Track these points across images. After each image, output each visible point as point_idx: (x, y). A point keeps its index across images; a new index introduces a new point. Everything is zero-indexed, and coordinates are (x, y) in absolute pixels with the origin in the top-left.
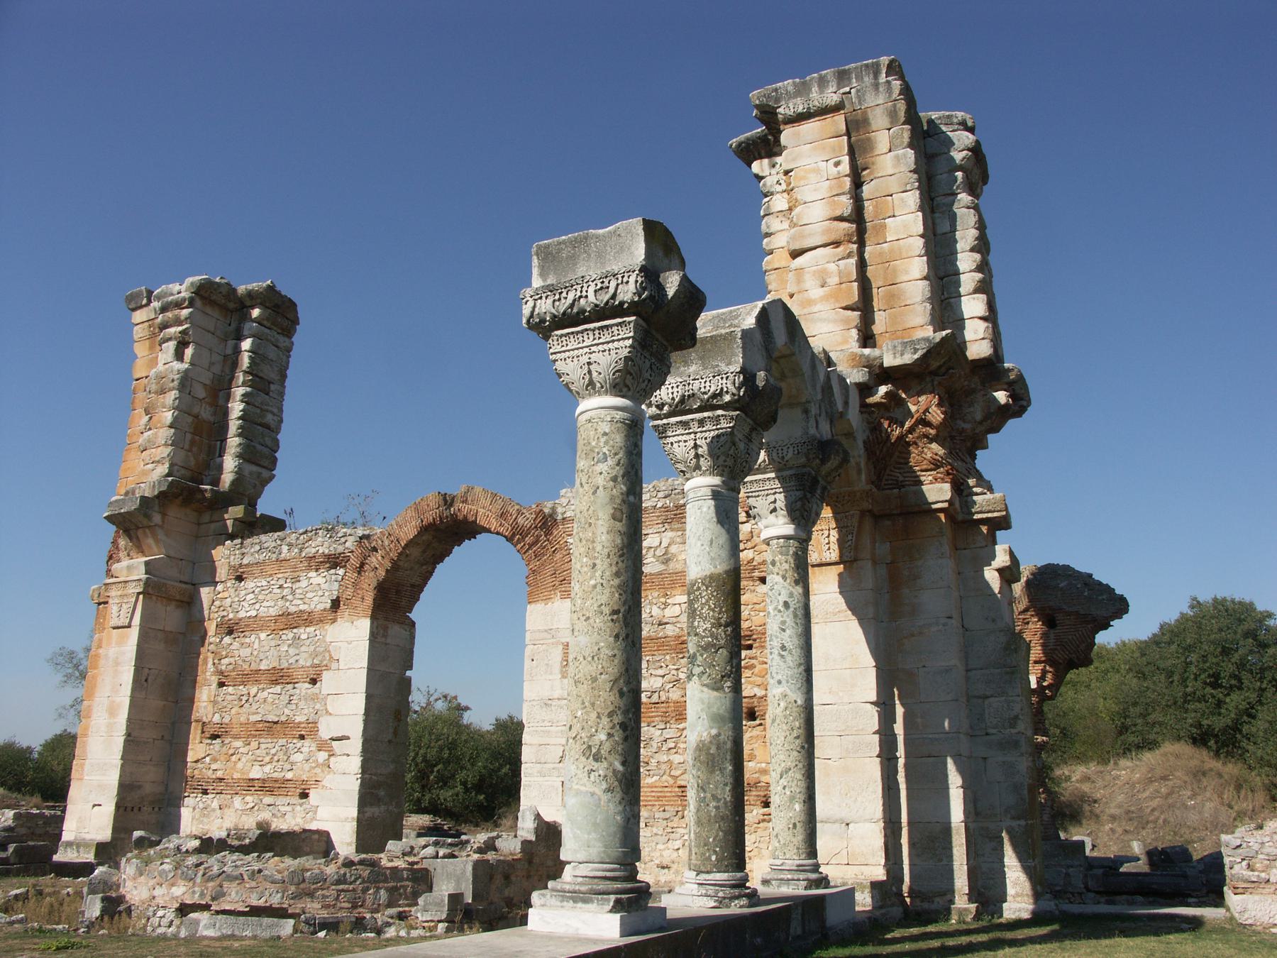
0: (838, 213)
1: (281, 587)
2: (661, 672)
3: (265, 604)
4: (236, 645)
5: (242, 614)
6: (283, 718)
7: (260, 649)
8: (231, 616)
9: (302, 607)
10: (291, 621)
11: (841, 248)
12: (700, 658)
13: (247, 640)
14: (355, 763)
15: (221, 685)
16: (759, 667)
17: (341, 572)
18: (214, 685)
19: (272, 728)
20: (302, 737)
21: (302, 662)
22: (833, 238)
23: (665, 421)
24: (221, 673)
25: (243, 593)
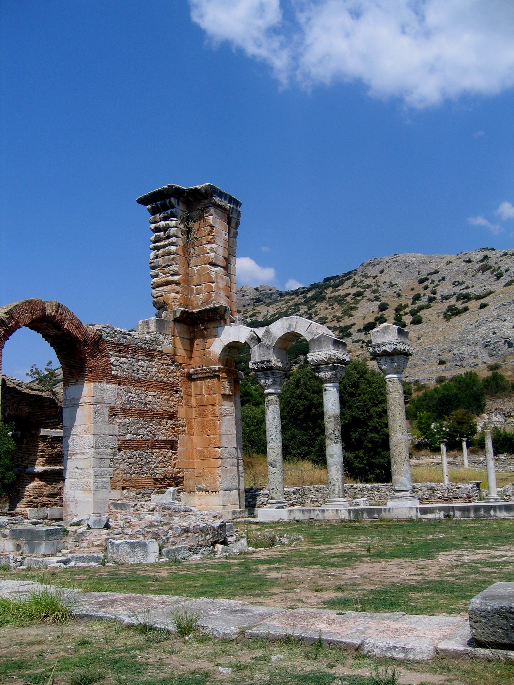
2: (146, 426)
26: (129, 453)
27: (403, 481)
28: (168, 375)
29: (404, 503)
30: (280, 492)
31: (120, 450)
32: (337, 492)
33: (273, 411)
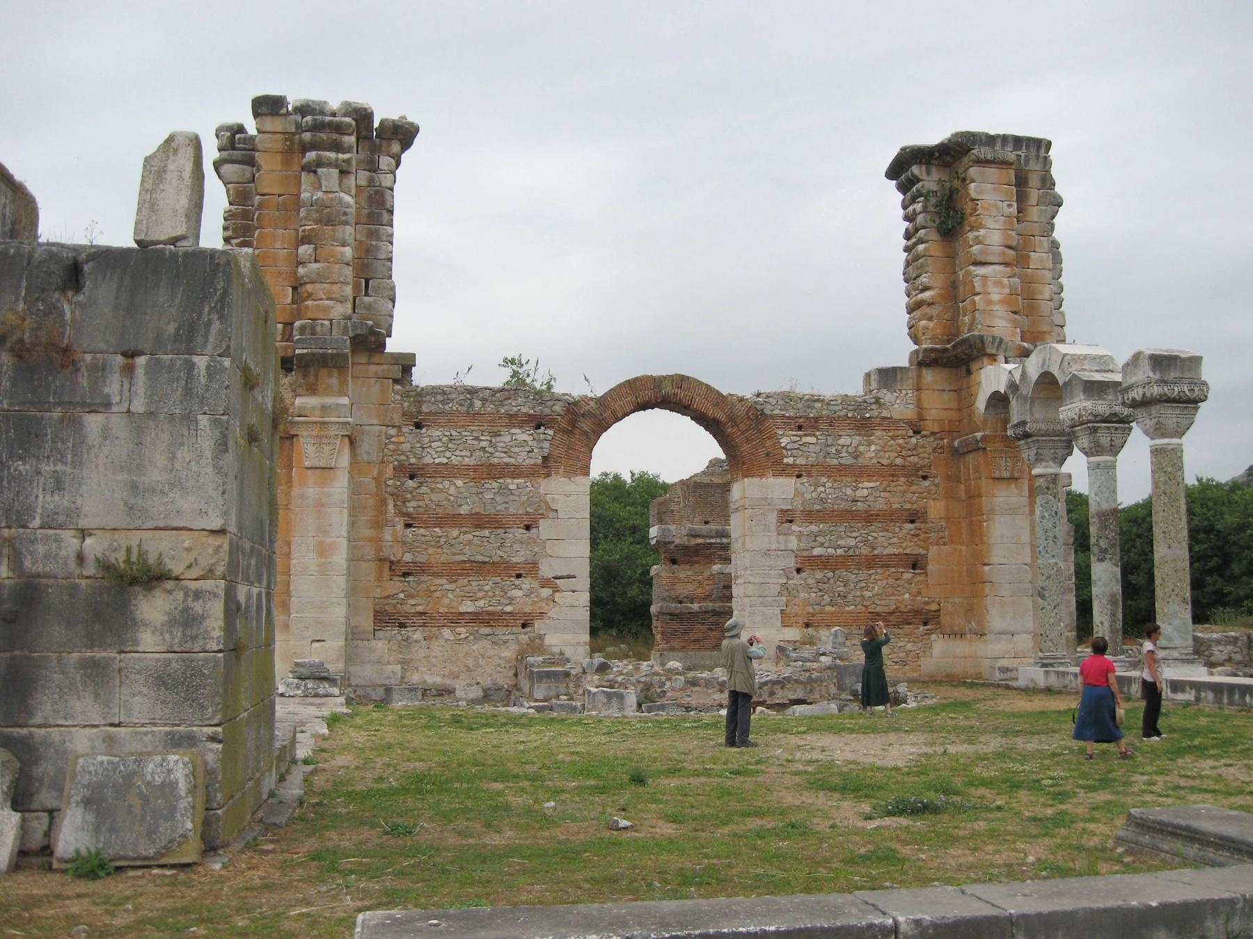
0: (1010, 243)
1: (477, 438)
2: (854, 535)
3: (458, 453)
4: (424, 489)
5: (427, 460)
6: (496, 559)
7: (455, 494)
8: (413, 460)
9: (506, 460)
10: (491, 471)
13: (440, 486)
14: (584, 598)
15: (408, 526)
16: (923, 536)
17: (551, 432)
18: (400, 527)
19: (482, 568)
20: (519, 576)
21: (512, 510)
22: (1007, 260)
24: (408, 515)
25: (427, 440)
26: (819, 575)
28: (904, 453)
31: (799, 571)
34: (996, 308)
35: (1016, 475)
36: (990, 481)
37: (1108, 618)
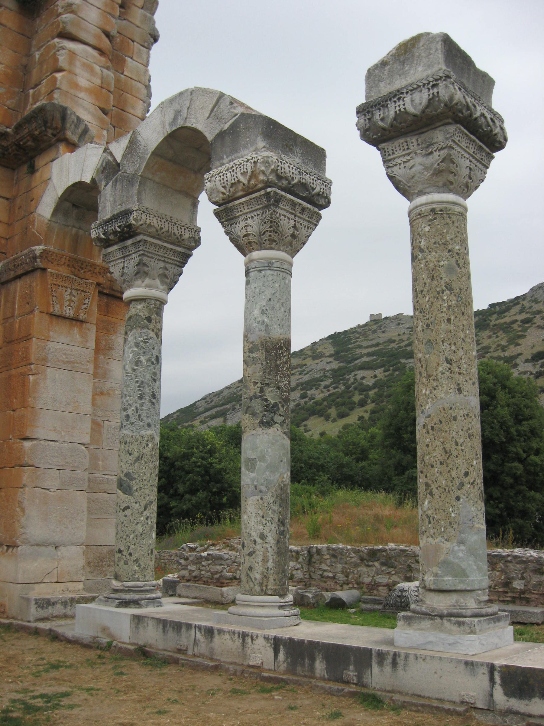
0: (108, 28)
11: (103, 59)
12: (281, 408)
22: (102, 46)
23: (283, 193)
27: (451, 558)
29: (451, 639)
30: (136, 561)
32: (258, 576)
33: (137, 345)
34: (82, 95)
35: (82, 316)
36: (47, 317)
37: (274, 527)
